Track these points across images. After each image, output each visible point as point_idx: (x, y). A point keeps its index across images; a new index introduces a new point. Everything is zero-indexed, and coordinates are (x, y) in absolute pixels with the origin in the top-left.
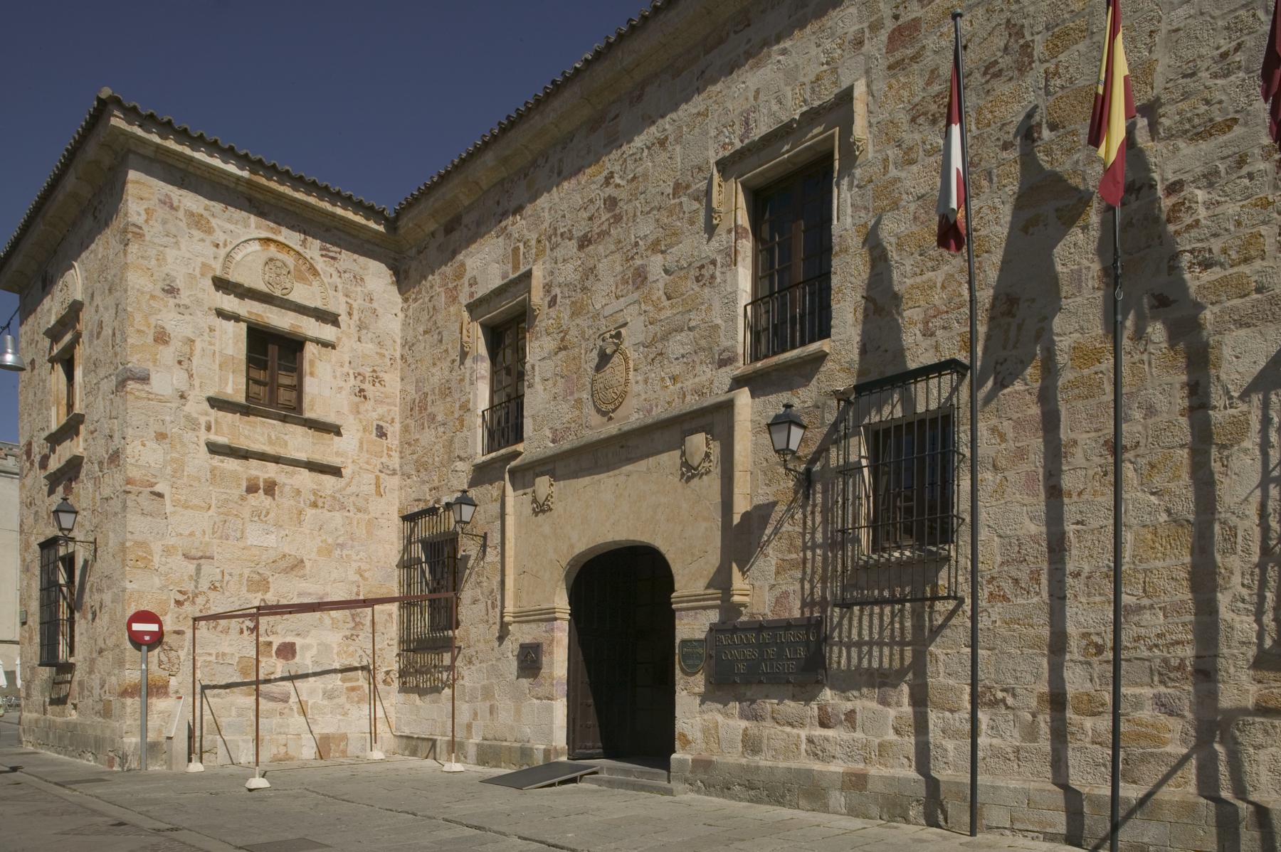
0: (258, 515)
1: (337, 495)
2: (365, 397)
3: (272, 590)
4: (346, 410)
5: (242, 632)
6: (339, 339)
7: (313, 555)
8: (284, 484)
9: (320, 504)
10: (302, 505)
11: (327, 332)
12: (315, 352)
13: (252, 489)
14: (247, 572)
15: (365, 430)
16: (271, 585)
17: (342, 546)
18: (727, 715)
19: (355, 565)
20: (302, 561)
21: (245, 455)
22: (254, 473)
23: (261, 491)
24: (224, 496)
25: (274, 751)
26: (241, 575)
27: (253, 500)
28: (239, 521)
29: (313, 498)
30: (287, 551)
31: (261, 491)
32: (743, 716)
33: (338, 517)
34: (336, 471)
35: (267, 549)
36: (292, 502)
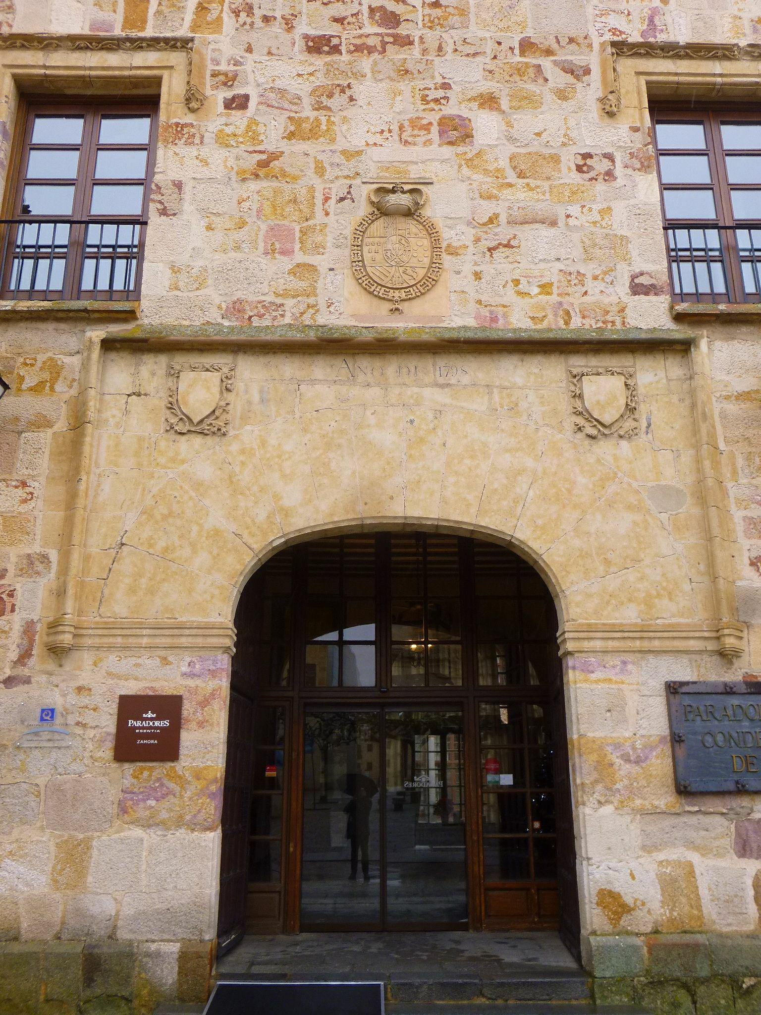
18: (704, 850)
32: (744, 849)
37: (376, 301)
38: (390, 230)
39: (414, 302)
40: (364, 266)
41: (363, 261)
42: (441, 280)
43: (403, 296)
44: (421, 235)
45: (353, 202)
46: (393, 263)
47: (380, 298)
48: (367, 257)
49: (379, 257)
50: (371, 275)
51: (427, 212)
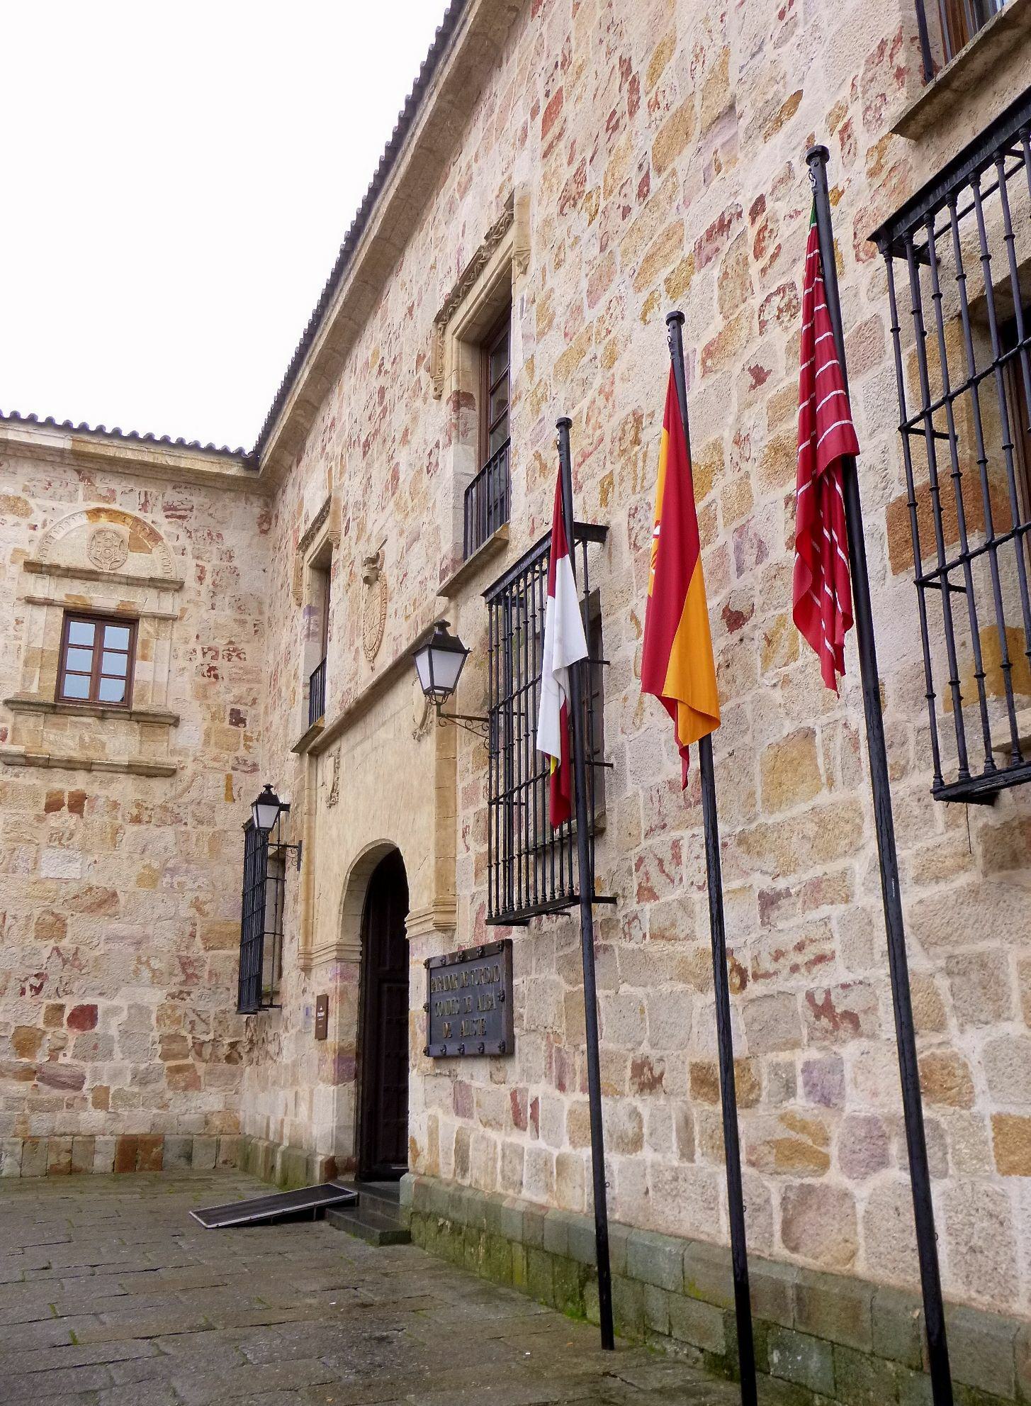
0: (58, 838)
1: (169, 805)
2: (216, 677)
3: (69, 935)
4: (188, 695)
5: (23, 992)
6: (183, 610)
7: (131, 886)
8: (97, 797)
9: (146, 818)
10: (120, 821)
11: (167, 604)
12: (151, 630)
13: (53, 805)
14: (37, 912)
15: (213, 718)
16: (69, 928)
17: (173, 871)
19: (190, 896)
20: (114, 895)
21: (48, 764)
22: (57, 786)
23: (65, 808)
24: (16, 818)
25: (52, 1159)
26: (28, 918)
27: (54, 820)
28: (33, 848)
29: (135, 811)
30: (94, 883)
31: (65, 808)
33: (169, 834)
34: (170, 773)
35: (67, 882)
36: (106, 819)
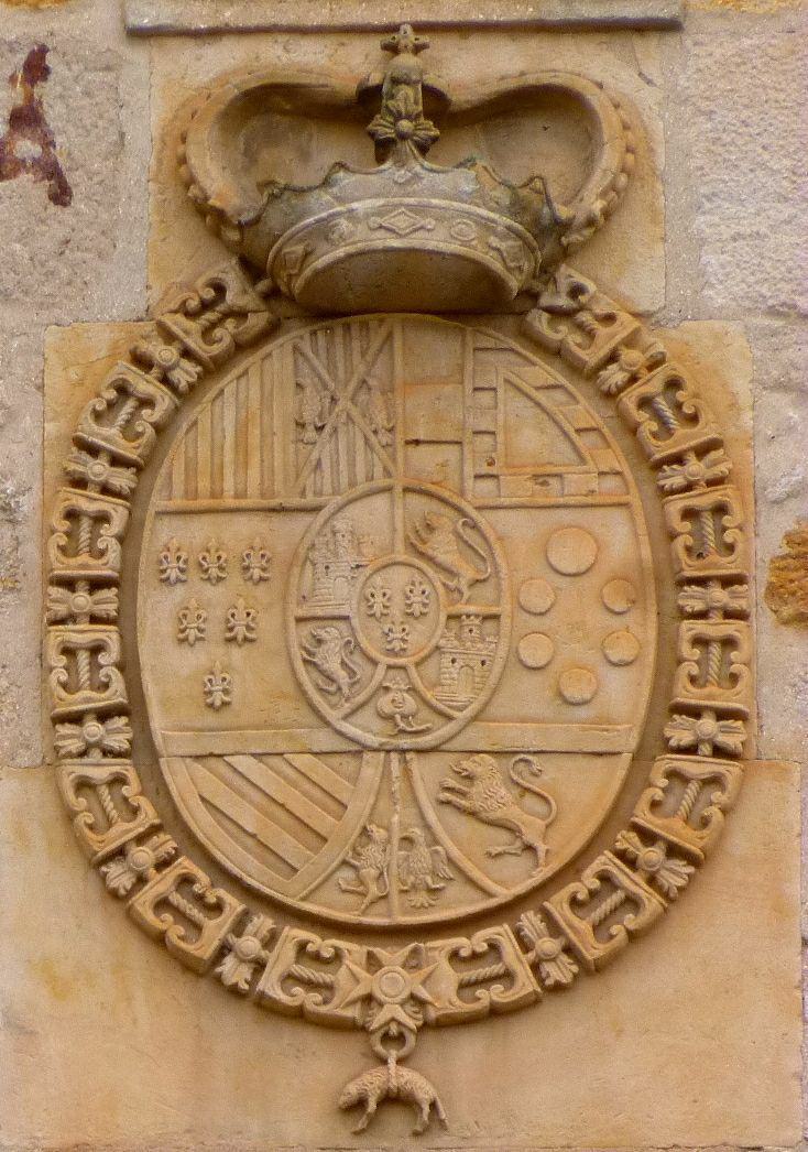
37: (233, 1032)
38: (346, 455)
39: (530, 1040)
40: (143, 750)
41: (132, 709)
42: (741, 842)
43: (445, 994)
44: (578, 482)
45: (61, 195)
46: (366, 729)
47: (268, 1009)
48: (169, 670)
49: (254, 678)
50: (202, 823)
51: (633, 277)
